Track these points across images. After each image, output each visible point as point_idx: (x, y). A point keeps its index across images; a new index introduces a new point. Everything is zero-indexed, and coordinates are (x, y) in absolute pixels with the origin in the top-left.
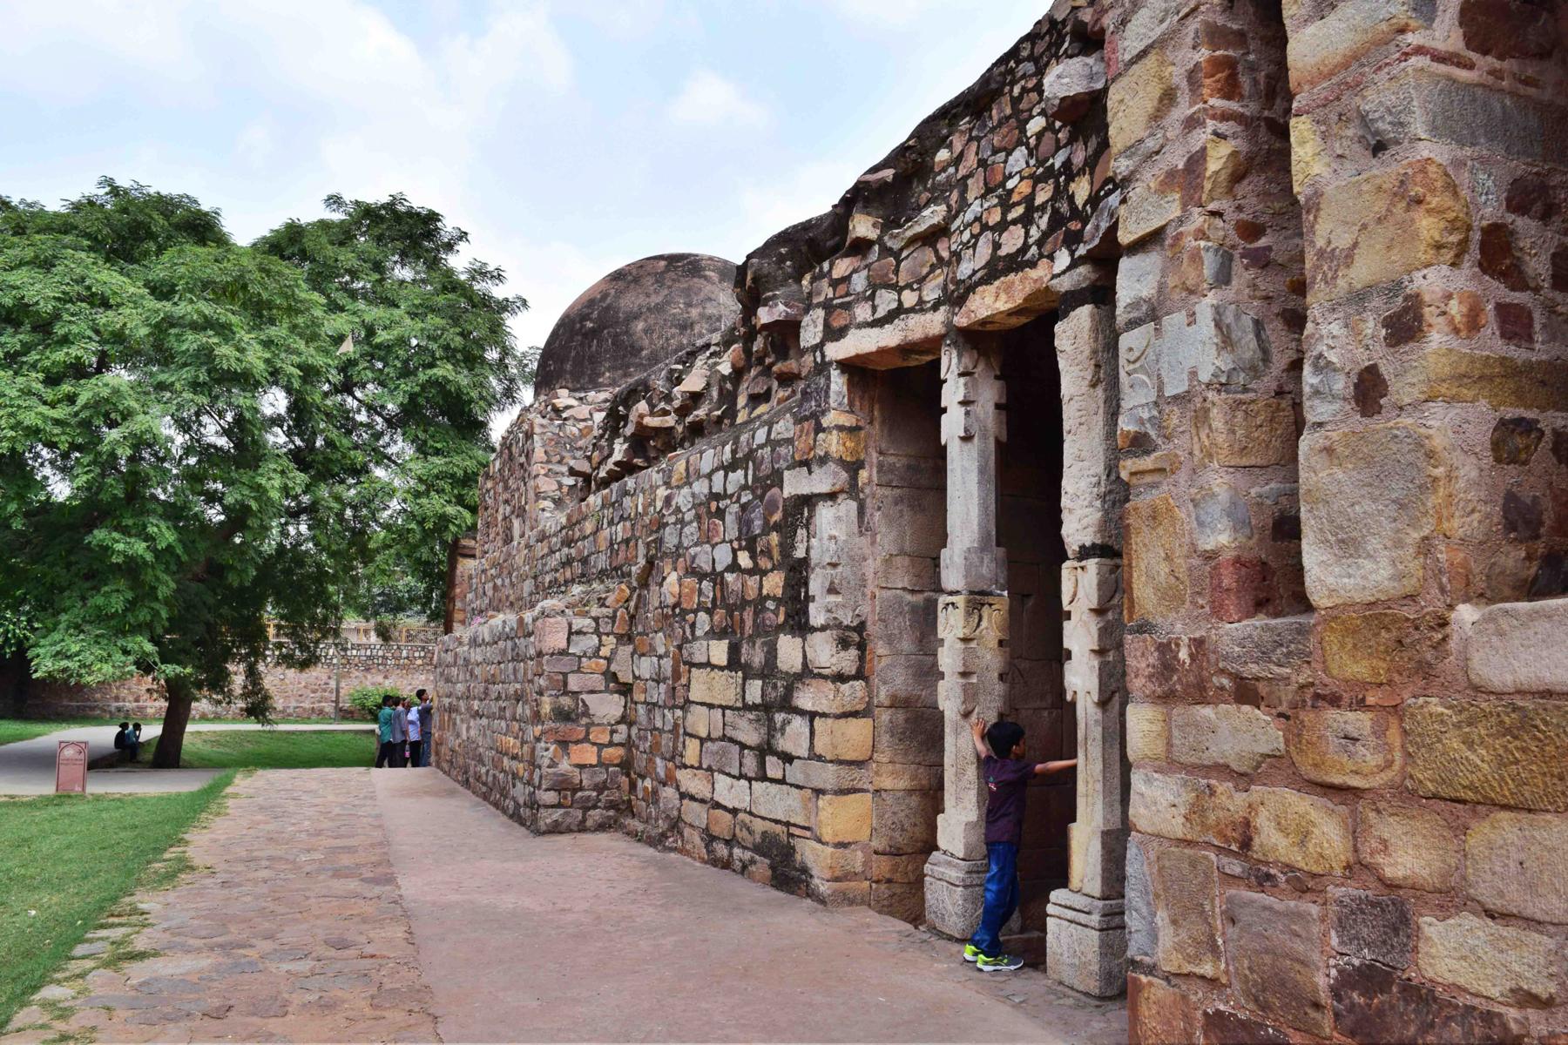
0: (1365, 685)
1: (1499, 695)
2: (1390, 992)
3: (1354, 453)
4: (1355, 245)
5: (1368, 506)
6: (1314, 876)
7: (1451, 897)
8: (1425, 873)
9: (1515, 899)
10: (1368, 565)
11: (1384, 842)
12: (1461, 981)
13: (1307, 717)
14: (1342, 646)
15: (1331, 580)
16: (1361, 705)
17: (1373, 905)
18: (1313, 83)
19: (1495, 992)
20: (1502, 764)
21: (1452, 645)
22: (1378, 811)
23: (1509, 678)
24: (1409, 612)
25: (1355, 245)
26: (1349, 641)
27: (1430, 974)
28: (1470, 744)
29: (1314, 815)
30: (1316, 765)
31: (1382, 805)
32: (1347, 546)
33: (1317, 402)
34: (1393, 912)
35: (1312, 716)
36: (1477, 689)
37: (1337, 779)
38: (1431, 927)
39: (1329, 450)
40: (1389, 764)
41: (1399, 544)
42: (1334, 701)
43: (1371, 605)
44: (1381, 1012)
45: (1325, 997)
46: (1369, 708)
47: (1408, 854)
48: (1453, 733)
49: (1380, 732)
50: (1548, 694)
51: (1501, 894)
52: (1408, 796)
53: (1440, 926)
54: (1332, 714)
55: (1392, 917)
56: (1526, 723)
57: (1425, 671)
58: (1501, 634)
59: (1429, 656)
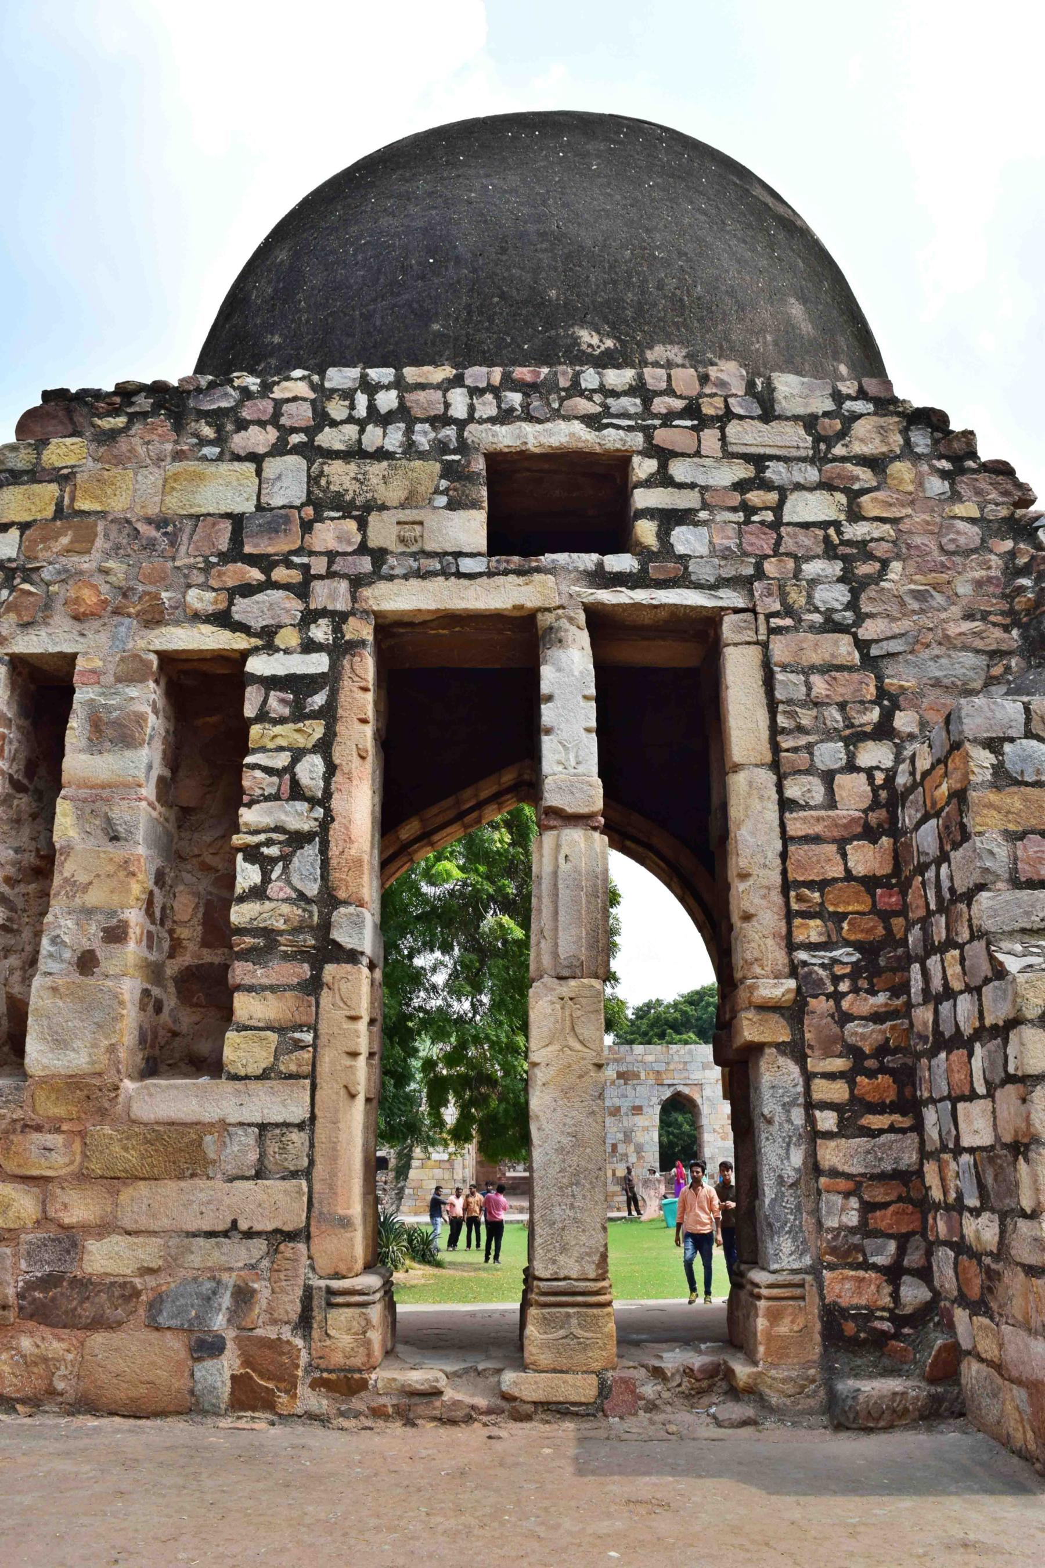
0: (61, 1120)
1: (146, 1125)
2: (61, 1286)
3: (72, 993)
4: (91, 883)
5: (77, 1023)
6: (10, 1230)
7: (104, 1229)
8: (91, 1218)
9: (144, 1223)
10: (72, 1055)
11: (65, 1206)
12: (109, 1270)
13: (16, 1138)
14: (48, 1098)
15: (45, 1061)
16: (58, 1130)
17: (53, 1240)
18: (79, 787)
19: (128, 1272)
20: (143, 1157)
21: (120, 1099)
22: (63, 1188)
23: (152, 1116)
24: (97, 1082)
25: (91, 883)
26: (53, 1096)
27: (90, 1270)
28: (126, 1149)
29: (14, 1195)
30: (19, 1166)
31: (65, 1185)
32: (59, 1042)
33: (49, 961)
34: (69, 1240)
35: (20, 1137)
36: (134, 1122)
37: (35, 1172)
38: (92, 1246)
39: (54, 989)
40: (72, 1162)
41: (95, 1046)
42: (38, 1129)
43: (71, 1076)
44: (53, 1299)
45: (12, 1300)
46: (63, 1132)
47: (78, 1208)
48: (116, 1143)
49: (68, 1145)
50: (173, 1124)
51: (136, 1222)
52: (83, 1178)
53: (98, 1244)
54: (35, 1136)
55: (66, 1245)
56: (159, 1137)
57: (103, 1113)
58: (151, 1095)
59: (107, 1105)
